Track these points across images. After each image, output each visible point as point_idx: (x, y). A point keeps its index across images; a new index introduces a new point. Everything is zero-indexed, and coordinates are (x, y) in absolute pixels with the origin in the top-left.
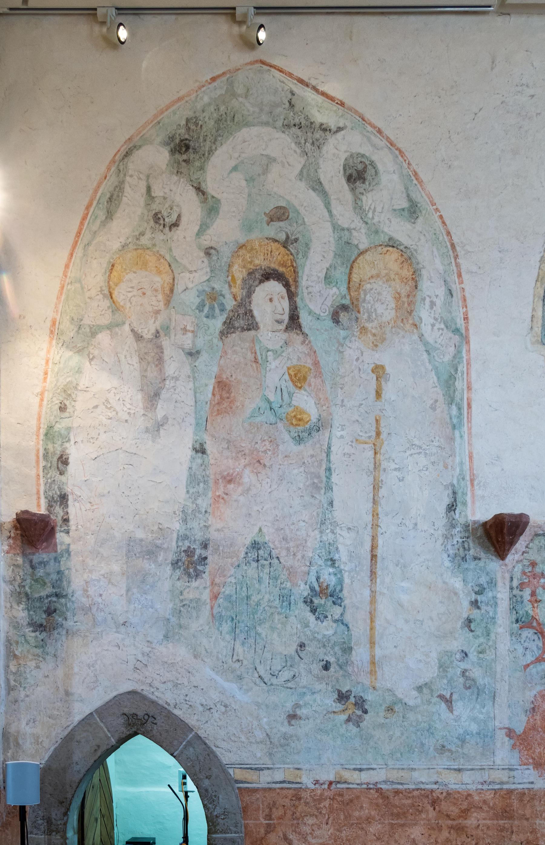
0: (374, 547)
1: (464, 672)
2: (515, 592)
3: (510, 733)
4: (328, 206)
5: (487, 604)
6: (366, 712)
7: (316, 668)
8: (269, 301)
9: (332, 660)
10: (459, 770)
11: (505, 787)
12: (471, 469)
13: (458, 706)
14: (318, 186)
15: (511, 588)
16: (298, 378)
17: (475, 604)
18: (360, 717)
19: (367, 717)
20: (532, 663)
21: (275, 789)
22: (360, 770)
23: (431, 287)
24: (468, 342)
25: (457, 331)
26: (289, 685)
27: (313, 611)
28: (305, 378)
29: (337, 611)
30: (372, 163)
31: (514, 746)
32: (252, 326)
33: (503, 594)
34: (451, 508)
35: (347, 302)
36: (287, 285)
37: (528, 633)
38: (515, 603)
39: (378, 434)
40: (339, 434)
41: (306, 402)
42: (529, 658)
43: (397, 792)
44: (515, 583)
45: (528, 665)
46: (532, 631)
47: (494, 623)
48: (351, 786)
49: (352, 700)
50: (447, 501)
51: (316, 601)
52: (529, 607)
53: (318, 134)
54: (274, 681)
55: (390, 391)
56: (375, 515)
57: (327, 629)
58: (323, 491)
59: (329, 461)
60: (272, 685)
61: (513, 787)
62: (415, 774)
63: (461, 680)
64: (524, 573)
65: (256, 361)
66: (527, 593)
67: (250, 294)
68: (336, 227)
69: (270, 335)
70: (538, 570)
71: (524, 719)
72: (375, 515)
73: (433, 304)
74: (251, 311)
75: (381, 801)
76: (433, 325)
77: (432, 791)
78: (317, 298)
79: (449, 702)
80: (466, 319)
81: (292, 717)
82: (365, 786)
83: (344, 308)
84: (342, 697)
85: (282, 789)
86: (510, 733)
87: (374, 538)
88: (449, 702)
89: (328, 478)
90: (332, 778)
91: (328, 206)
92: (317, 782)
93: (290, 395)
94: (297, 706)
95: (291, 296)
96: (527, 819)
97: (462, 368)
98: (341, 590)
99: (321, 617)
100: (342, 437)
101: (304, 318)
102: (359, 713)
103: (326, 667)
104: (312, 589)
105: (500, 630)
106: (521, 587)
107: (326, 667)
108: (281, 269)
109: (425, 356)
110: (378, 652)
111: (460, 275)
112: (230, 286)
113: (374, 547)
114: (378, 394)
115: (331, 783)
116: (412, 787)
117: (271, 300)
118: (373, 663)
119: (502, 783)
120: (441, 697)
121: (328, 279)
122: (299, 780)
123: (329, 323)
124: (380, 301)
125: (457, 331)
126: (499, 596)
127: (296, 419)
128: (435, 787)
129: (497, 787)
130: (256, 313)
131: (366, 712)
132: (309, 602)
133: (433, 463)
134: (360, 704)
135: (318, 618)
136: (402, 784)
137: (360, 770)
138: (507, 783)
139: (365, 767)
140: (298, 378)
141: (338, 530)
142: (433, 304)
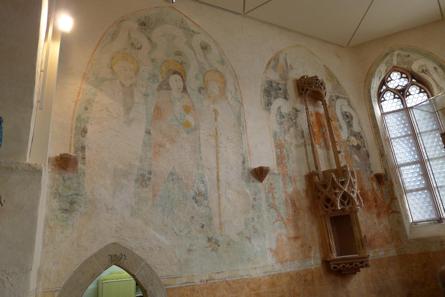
0: (218, 176)
1: (253, 226)
2: (267, 194)
3: (271, 250)
4: (195, 54)
5: (259, 199)
6: (219, 246)
7: (198, 227)
8: (175, 81)
9: (204, 223)
10: (255, 268)
11: (272, 273)
12: (249, 149)
13: (253, 240)
14: (191, 48)
15: (266, 193)
16: (187, 110)
17: (255, 199)
18: (217, 248)
19: (219, 248)
20: (275, 221)
21: (183, 287)
22: (219, 273)
23: (230, 87)
24: (243, 106)
25: (239, 102)
26: (188, 235)
27: (197, 202)
28: (189, 110)
29: (206, 202)
30: (209, 45)
31: (273, 256)
32: (169, 89)
33: (263, 195)
34: (244, 162)
35: (203, 86)
36: (182, 77)
37: (272, 210)
38: (267, 198)
39: (217, 133)
40: (203, 132)
41: (190, 119)
42: (274, 220)
43: (234, 281)
44: (267, 191)
45: (274, 223)
46: (274, 209)
47: (262, 206)
48: (215, 281)
49: (214, 241)
50: (241, 160)
51: (197, 198)
52: (272, 200)
53: (191, 33)
54: (181, 234)
55: (219, 119)
56: (218, 164)
57: (202, 210)
58: (198, 153)
59: (199, 142)
60: (180, 236)
61: (274, 273)
62: (240, 272)
63: (253, 230)
64: (269, 187)
65: (171, 101)
66: (271, 195)
67: (168, 78)
68: (198, 62)
69: (176, 93)
70: (273, 186)
71: (275, 244)
72: (218, 164)
73: (231, 92)
74: (169, 83)
75: (227, 286)
76: (232, 99)
77: (247, 279)
78: (193, 84)
79: (249, 239)
80: (242, 98)
81: (190, 250)
82: (221, 280)
83: (202, 88)
84: (210, 240)
85: (186, 286)
86: (271, 250)
87: (218, 173)
88: (249, 239)
89: (200, 148)
90: (207, 278)
91: (195, 54)
92: (201, 281)
93: (184, 116)
94: (191, 245)
95: (184, 81)
96: (280, 286)
97: (242, 114)
98: (207, 194)
99: (200, 205)
100: (204, 133)
101: (188, 89)
102: (217, 246)
103: (202, 227)
104: (195, 193)
105: (264, 209)
106: (269, 192)
107: (202, 227)
108: (180, 71)
109: (230, 108)
110: (222, 220)
111: (238, 85)
112: (161, 74)
113: (218, 176)
114: (216, 120)
115: (207, 281)
116: (239, 278)
117: (176, 81)
118: (221, 224)
119: (271, 272)
120: (246, 237)
121: (196, 77)
122: (193, 281)
123: (197, 92)
124: (214, 88)
125: (239, 102)
126: (262, 196)
127: (187, 125)
128: (247, 277)
129: (269, 274)
130: (170, 84)
131: (219, 246)
132: (194, 198)
133: (236, 146)
134: (217, 242)
135: (198, 205)
136: (235, 277)
137: (219, 273)
138: (272, 271)
139: (220, 271)
140: (187, 110)
141: (204, 169)
142: (231, 92)
